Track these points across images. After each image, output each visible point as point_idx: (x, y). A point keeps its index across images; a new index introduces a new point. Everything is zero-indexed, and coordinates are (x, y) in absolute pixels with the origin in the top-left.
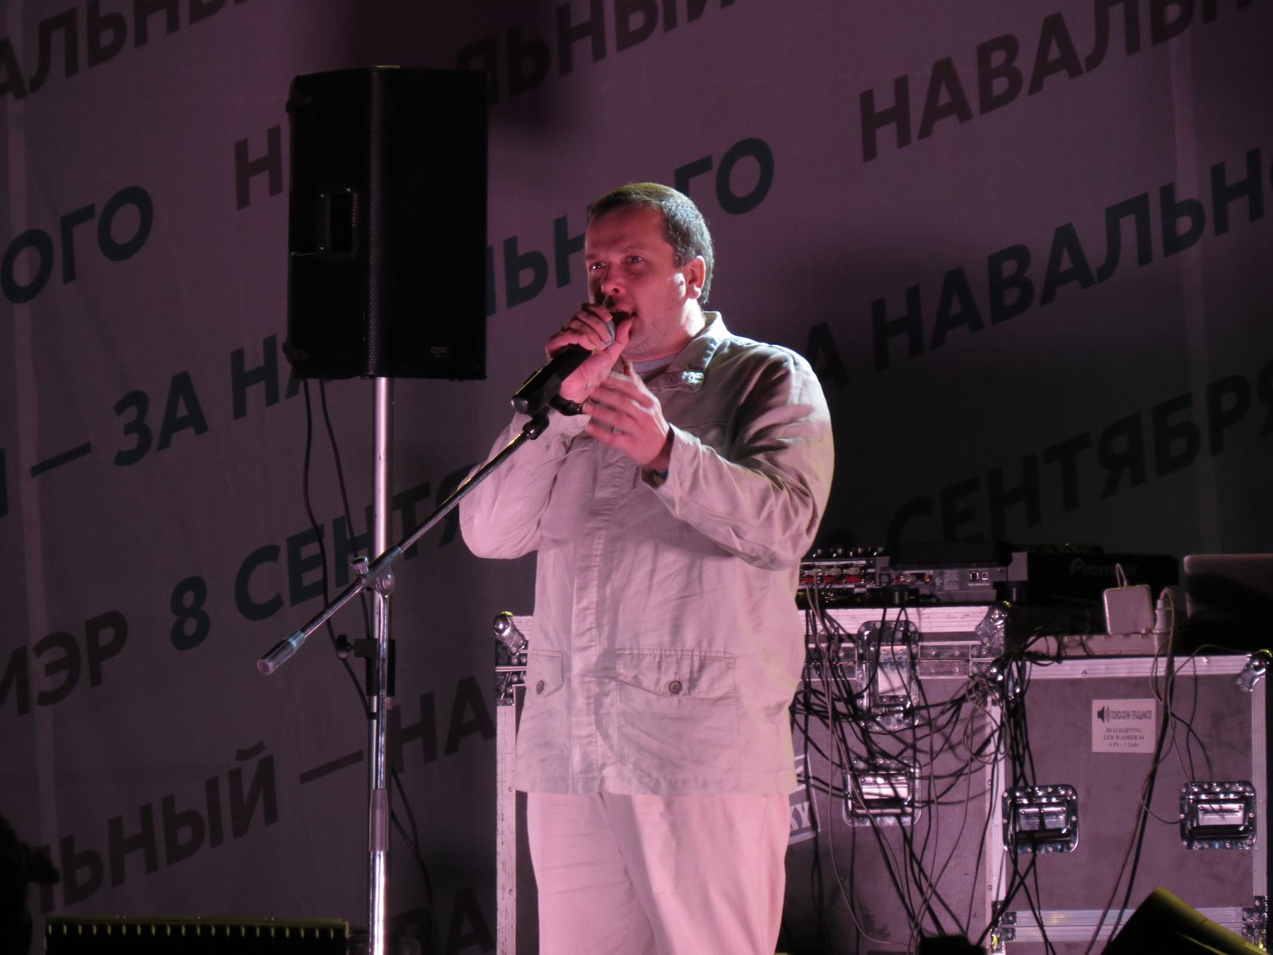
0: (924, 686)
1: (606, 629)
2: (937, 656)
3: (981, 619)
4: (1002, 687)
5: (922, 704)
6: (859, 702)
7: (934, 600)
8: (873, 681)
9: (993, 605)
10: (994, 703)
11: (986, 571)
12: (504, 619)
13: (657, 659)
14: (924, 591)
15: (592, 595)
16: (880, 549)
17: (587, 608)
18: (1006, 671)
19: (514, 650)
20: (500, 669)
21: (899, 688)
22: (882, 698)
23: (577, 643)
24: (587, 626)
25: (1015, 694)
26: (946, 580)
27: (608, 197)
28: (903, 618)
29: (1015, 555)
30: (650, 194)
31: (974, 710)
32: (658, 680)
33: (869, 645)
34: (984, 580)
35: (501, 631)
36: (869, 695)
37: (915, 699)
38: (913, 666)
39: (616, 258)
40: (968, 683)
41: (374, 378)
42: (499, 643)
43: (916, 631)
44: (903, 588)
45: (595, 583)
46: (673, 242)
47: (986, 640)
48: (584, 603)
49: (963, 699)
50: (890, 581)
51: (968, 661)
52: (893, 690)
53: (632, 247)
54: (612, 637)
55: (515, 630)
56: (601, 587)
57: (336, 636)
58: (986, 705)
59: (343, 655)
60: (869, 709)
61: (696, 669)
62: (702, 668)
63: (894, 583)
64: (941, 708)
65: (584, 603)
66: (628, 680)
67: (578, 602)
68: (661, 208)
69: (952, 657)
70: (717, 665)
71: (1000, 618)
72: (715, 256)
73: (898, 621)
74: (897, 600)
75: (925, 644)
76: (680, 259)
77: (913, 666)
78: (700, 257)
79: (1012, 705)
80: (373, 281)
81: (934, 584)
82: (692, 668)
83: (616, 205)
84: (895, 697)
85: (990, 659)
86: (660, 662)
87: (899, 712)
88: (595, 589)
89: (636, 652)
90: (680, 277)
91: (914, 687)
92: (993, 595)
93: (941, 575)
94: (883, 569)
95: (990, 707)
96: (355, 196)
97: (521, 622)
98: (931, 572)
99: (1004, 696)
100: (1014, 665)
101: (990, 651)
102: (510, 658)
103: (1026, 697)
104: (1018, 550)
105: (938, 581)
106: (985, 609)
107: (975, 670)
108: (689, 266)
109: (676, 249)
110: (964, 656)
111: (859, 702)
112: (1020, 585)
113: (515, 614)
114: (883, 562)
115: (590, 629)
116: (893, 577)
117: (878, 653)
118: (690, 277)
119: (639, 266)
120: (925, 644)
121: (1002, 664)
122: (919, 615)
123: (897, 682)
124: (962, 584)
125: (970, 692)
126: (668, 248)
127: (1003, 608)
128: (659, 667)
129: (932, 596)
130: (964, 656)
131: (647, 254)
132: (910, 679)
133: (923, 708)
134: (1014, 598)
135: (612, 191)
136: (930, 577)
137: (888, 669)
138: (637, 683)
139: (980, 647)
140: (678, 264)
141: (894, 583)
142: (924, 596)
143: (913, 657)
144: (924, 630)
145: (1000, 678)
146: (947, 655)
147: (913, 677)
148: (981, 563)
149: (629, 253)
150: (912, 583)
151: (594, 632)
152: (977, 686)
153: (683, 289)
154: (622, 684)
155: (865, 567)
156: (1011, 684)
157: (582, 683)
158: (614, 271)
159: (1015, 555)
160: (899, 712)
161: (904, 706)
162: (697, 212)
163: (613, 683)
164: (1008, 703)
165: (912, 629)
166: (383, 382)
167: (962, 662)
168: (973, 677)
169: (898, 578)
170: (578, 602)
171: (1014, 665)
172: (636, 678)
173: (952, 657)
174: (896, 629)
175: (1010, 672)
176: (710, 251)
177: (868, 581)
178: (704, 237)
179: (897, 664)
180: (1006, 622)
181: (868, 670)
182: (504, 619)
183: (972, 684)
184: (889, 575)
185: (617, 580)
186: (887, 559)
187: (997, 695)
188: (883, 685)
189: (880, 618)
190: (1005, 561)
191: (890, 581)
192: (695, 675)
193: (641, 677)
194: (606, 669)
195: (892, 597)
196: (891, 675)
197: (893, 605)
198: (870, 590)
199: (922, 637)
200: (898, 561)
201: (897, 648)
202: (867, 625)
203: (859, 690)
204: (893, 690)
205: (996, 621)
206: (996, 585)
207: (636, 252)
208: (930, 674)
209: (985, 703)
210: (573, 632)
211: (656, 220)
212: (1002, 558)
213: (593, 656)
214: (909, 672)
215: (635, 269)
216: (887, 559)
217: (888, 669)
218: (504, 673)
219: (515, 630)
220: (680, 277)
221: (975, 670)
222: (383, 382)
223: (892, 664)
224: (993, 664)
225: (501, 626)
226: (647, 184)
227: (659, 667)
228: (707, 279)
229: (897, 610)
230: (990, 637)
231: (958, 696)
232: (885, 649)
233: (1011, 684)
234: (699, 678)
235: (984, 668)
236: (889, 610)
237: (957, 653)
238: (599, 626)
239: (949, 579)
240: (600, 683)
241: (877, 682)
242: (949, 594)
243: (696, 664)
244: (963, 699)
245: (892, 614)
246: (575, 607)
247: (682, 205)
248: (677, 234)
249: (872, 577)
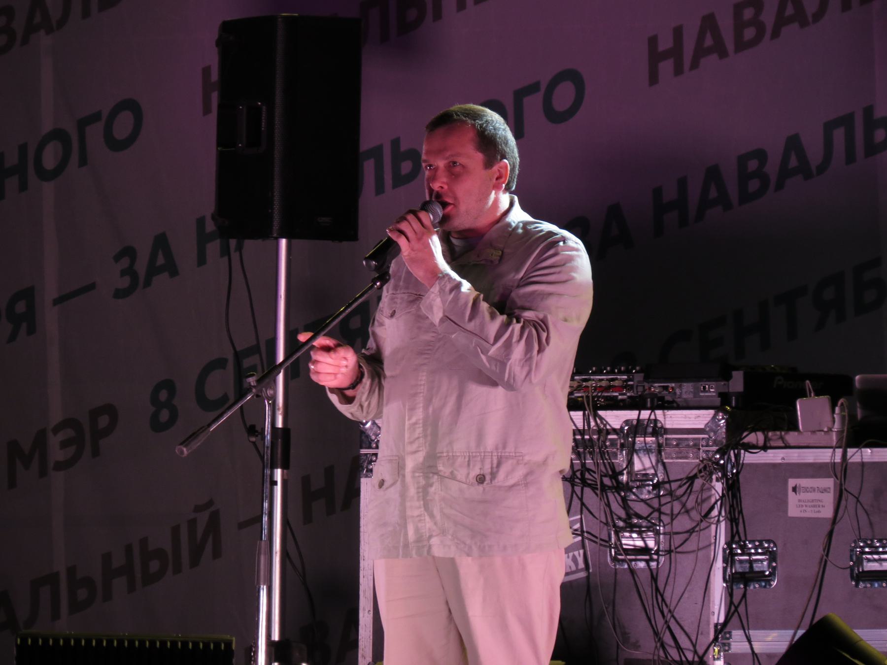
0: (667, 465)
2: (677, 445)
3: (709, 419)
4: (723, 468)
5: (666, 480)
6: (621, 478)
7: (675, 405)
8: (630, 463)
9: (717, 409)
10: (717, 480)
11: (713, 384)
15: (419, 414)
16: (638, 368)
17: (416, 423)
18: (726, 457)
21: (649, 468)
22: (637, 475)
24: (417, 436)
26: (684, 390)
28: (653, 417)
31: (703, 485)
34: (712, 391)
36: (628, 473)
37: (661, 476)
38: (659, 452)
39: (441, 163)
40: (699, 465)
43: (662, 427)
44: (653, 396)
45: (421, 405)
47: (712, 434)
48: (414, 420)
50: (644, 390)
51: (699, 449)
52: (645, 469)
53: (452, 156)
54: (434, 444)
56: (426, 408)
58: (711, 481)
60: (627, 483)
67: (409, 419)
69: (688, 446)
71: (723, 418)
73: (649, 419)
74: (649, 405)
75: (669, 436)
77: (659, 452)
81: (675, 393)
85: (715, 448)
87: (649, 485)
88: (421, 410)
91: (660, 467)
92: (718, 401)
93: (680, 387)
94: (639, 382)
98: (673, 385)
99: (725, 475)
101: (715, 443)
105: (678, 391)
106: (712, 412)
107: (704, 456)
108: (495, 168)
110: (696, 446)
111: (621, 478)
112: (738, 395)
114: (639, 377)
115: (418, 438)
116: (646, 388)
117: (634, 443)
119: (458, 169)
120: (669, 436)
122: (664, 415)
123: (648, 464)
124: (696, 393)
125: (700, 471)
126: (480, 156)
127: (725, 412)
130: (696, 446)
132: (657, 462)
133: (666, 483)
136: (673, 388)
137: (641, 455)
139: (708, 439)
142: (669, 402)
143: (660, 446)
145: (722, 462)
147: (660, 460)
148: (709, 378)
149: (451, 159)
150: (659, 392)
151: (421, 440)
152: (705, 467)
154: (442, 478)
155: (626, 381)
156: (729, 466)
157: (413, 477)
160: (649, 485)
161: (652, 481)
165: (659, 425)
167: (695, 450)
168: (702, 461)
169: (650, 389)
170: (409, 419)
175: (729, 458)
177: (628, 390)
179: (648, 451)
183: (702, 466)
187: (720, 474)
188: (637, 466)
189: (636, 417)
191: (644, 390)
194: (430, 467)
195: (646, 403)
197: (646, 408)
199: (667, 431)
200: (649, 376)
201: (649, 439)
202: (627, 422)
203: (621, 469)
204: (645, 469)
205: (720, 420)
206: (721, 395)
208: (672, 458)
210: (406, 440)
213: (420, 457)
214: (657, 456)
215: (455, 171)
217: (641, 455)
221: (704, 456)
223: (644, 450)
224: (717, 452)
229: (649, 412)
230: (715, 432)
231: (691, 475)
232: (639, 440)
233: (729, 466)
235: (710, 454)
236: (643, 412)
237: (691, 443)
238: (425, 436)
239: (686, 390)
240: (426, 477)
241: (633, 464)
242: (686, 400)
245: (645, 414)
246: (407, 423)
249: (631, 388)
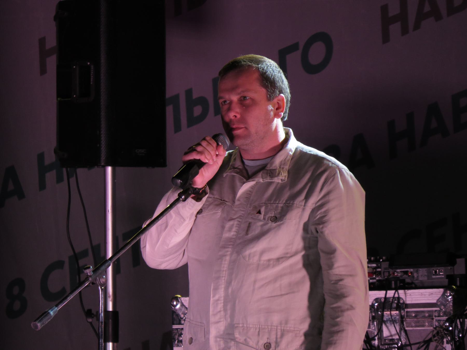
0: (408, 332)
1: (229, 312)
2: (416, 316)
3: (439, 296)
4: (452, 333)
5: (408, 343)
6: (373, 342)
7: (413, 285)
8: (380, 331)
9: (446, 288)
10: (448, 343)
11: (442, 269)
12: (177, 299)
13: (257, 330)
14: (408, 280)
15: (221, 293)
16: (384, 258)
17: (218, 300)
18: (454, 325)
19: (182, 316)
20: (175, 327)
21: (395, 335)
22: (385, 340)
23: (212, 319)
24: (219, 310)
25: (459, 337)
26: (420, 274)
27: (229, 64)
28: (396, 295)
29: (458, 260)
30: (251, 60)
31: (437, 347)
32: (258, 342)
33: (378, 311)
34: (441, 274)
35: (175, 306)
36: (378, 339)
37: (404, 340)
38: (402, 322)
40: (433, 331)
41: (104, 167)
42: (174, 312)
43: (404, 303)
44: (397, 279)
45: (223, 286)
46: (266, 87)
47: (442, 307)
48: (217, 297)
49: (430, 340)
50: (389, 275)
51: (433, 319)
52: (391, 336)
54: (232, 316)
55: (182, 305)
56: (227, 288)
57: (86, 309)
58: (443, 343)
59: (90, 320)
60: (378, 346)
61: (279, 336)
62: (282, 336)
63: (391, 276)
64: (417, 345)
65: (217, 297)
66: (241, 341)
67: (214, 296)
68: (258, 69)
69: (424, 317)
70: (290, 334)
71: (450, 295)
72: (291, 93)
73: (394, 297)
74: (393, 286)
75: (409, 310)
76: (270, 96)
77: (402, 322)
78: (282, 95)
79: (458, 344)
80: (103, 114)
81: (413, 277)
82: (277, 336)
83: (234, 67)
84: (393, 340)
85: (445, 318)
86: (259, 332)
87: (395, 348)
88: (223, 290)
89: (245, 325)
90: (270, 107)
91: (403, 334)
92: (446, 282)
93: (417, 271)
94: (385, 269)
95: (445, 345)
96: (92, 67)
97: (185, 300)
98: (412, 270)
99: (453, 338)
100: (458, 321)
101: (445, 314)
102: (180, 321)
103: (465, 339)
104: (460, 257)
105: (415, 275)
106: (442, 290)
107: (437, 324)
109: (268, 91)
110: (431, 317)
111: (373, 342)
112: (461, 276)
113: (182, 296)
114: (385, 265)
115: (220, 311)
116: (391, 273)
117: (383, 315)
118: (277, 106)
120: (409, 310)
121: (451, 320)
122: (405, 294)
123: (393, 331)
124: (429, 277)
125: (434, 336)
127: (452, 290)
128: (259, 334)
129: (412, 283)
130: (431, 317)
131: (250, 95)
132: (401, 329)
133: (407, 345)
134: (458, 284)
135: (231, 60)
136: (411, 273)
137: (388, 324)
138: (246, 343)
139: (439, 311)
140: (269, 99)
141: (391, 276)
142: (408, 284)
143: (402, 317)
144: (408, 302)
145: (451, 328)
146: (421, 315)
147: (402, 328)
148: (439, 264)
150: (401, 276)
151: (222, 313)
152: (438, 333)
153: (272, 113)
154: (238, 343)
155: (375, 268)
156: (456, 332)
157: (216, 341)
158: (234, 105)
159: (458, 260)
160: (395, 348)
161: (397, 345)
162: (279, 69)
163: (233, 342)
164: (455, 342)
165: (401, 302)
166: (109, 169)
167: (430, 320)
168: (435, 328)
169: (394, 274)
170: (214, 296)
171: (458, 321)
172: (245, 340)
173: (424, 317)
174: (392, 302)
175: (456, 325)
176: (288, 90)
177: (377, 275)
178: (284, 83)
179: (393, 321)
180: (454, 297)
181: (377, 324)
182: (177, 299)
183: (435, 332)
184: (389, 272)
185: (234, 284)
186: (387, 263)
187: (449, 338)
188: (386, 333)
189: (383, 296)
190: (452, 263)
191: (389, 275)
192: (279, 340)
193: (248, 340)
194: (229, 334)
195: (390, 284)
196: (390, 327)
197: (391, 289)
198: (378, 281)
199: (407, 306)
200: (393, 264)
201: (394, 313)
202: (377, 300)
203: (373, 335)
204: (391, 336)
205: (448, 296)
206: (448, 277)
207: (245, 94)
208: (412, 327)
209: (443, 343)
210: (211, 313)
211: (256, 75)
212: (451, 261)
213: (222, 326)
214: (400, 325)
216: (387, 263)
217: (388, 324)
218: (177, 329)
219: (182, 305)
220: (270, 107)
221: (437, 324)
222: (109, 169)
223: (390, 321)
224: (447, 321)
225: (175, 303)
226: (251, 55)
227: (259, 334)
228: (286, 107)
229: (394, 291)
230: (445, 306)
231: (427, 339)
232: (387, 313)
233: (456, 332)
234: (281, 341)
235: (442, 323)
236: (389, 292)
237: (427, 315)
238: (225, 310)
239: (421, 274)
240: (226, 342)
241: (382, 331)
242: (421, 282)
243: (279, 334)
244: (430, 340)
245: (391, 293)
246: (212, 299)
247: (271, 66)
248: (268, 82)
249: (379, 274)
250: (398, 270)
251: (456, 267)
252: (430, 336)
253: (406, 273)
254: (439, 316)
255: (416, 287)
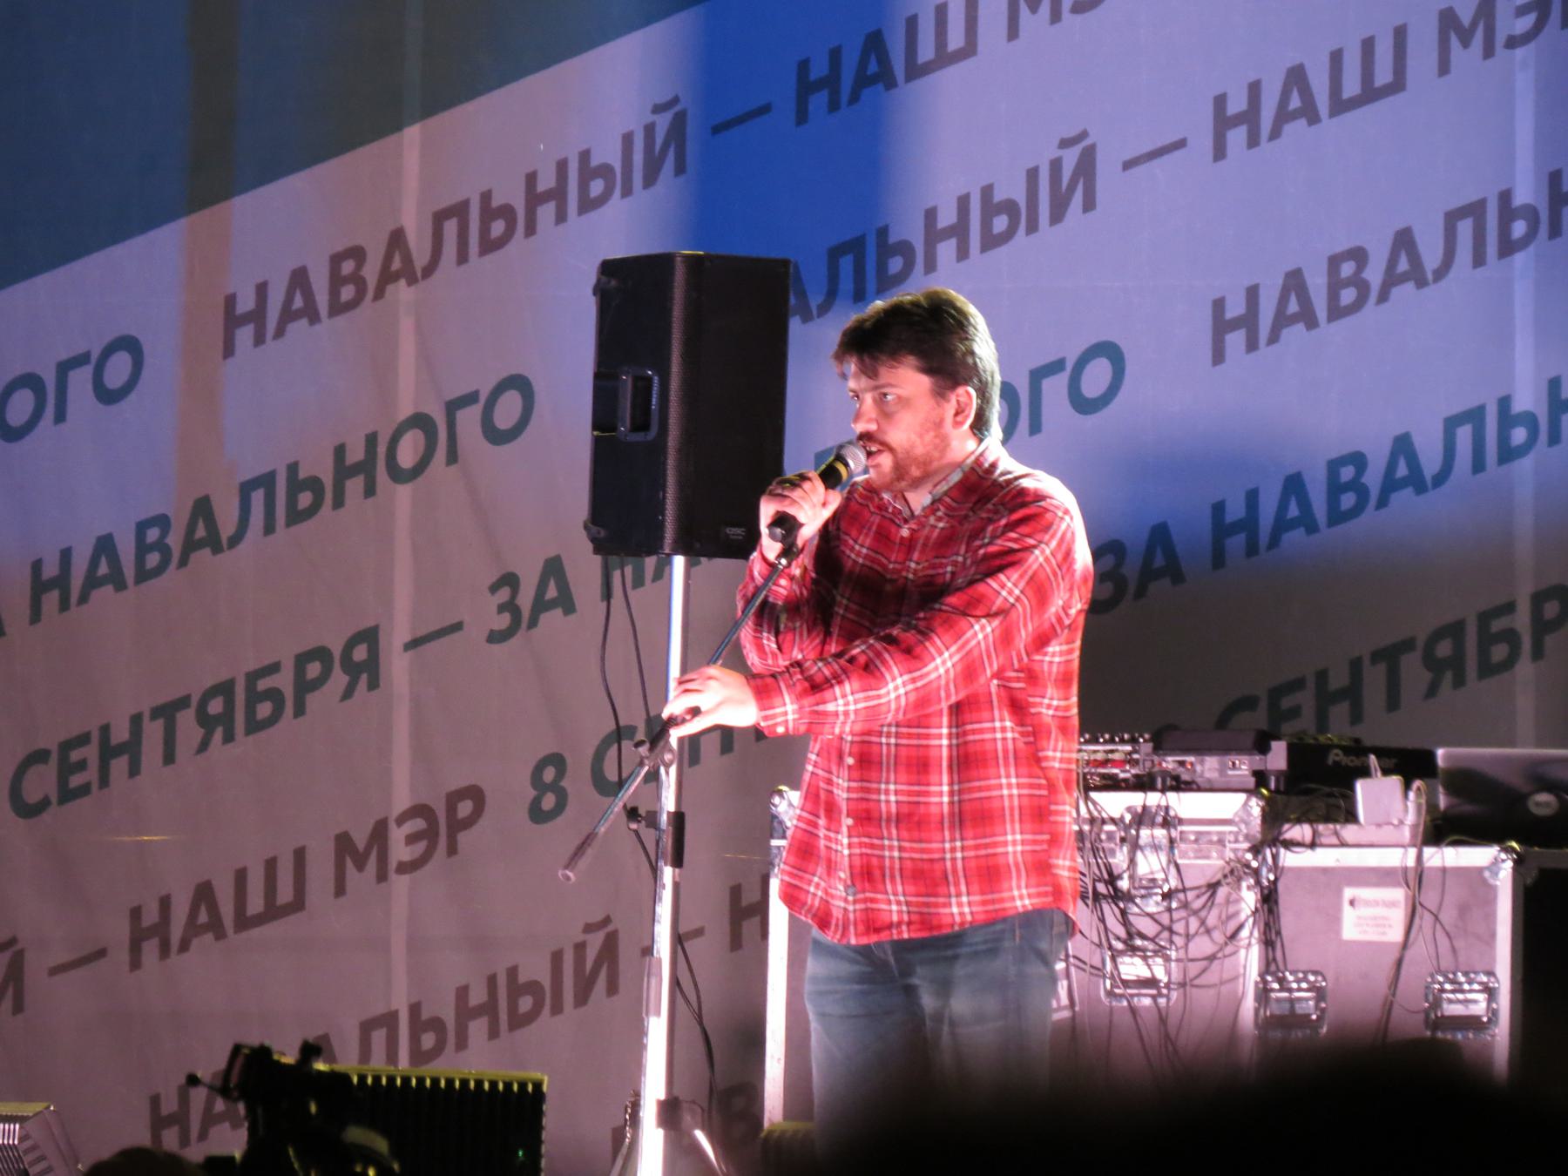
2: (1196, 841)
8: (1132, 861)
10: (1249, 888)
11: (1245, 759)
12: (780, 793)
14: (1185, 777)
28: (1163, 803)
34: (1243, 767)
36: (1131, 878)
37: (1174, 883)
44: (1165, 774)
47: (1243, 827)
69: (1211, 842)
74: (1159, 785)
80: (671, 462)
84: (1153, 880)
85: (1246, 845)
91: (1173, 870)
92: (1251, 782)
93: (1202, 763)
96: (656, 379)
99: (1258, 882)
101: (1247, 837)
103: (1280, 886)
104: (1278, 738)
105: (1198, 768)
106: (1242, 797)
112: (1279, 774)
114: (1147, 748)
117: (1138, 836)
123: (1157, 867)
124: (1222, 771)
125: (1225, 876)
129: (1193, 782)
134: (1273, 786)
139: (1236, 834)
143: (1172, 841)
147: (1172, 861)
148: (1240, 750)
152: (1232, 872)
155: (1130, 753)
164: (1262, 888)
165: (1172, 813)
166: (679, 562)
173: (1211, 842)
175: (1264, 859)
179: (1156, 847)
182: (780, 793)
183: (1227, 870)
190: (1262, 747)
199: (1181, 821)
209: (1239, 888)
216: (1150, 745)
217: (1148, 852)
221: (1232, 856)
230: (1246, 824)
232: (1145, 833)
233: (1264, 871)
237: (1215, 838)
239: (1209, 766)
242: (1209, 780)
250: (1170, 759)
251: (1270, 756)
252: (1219, 876)
253: (1182, 763)
254: (1236, 841)
255: (1199, 789)
